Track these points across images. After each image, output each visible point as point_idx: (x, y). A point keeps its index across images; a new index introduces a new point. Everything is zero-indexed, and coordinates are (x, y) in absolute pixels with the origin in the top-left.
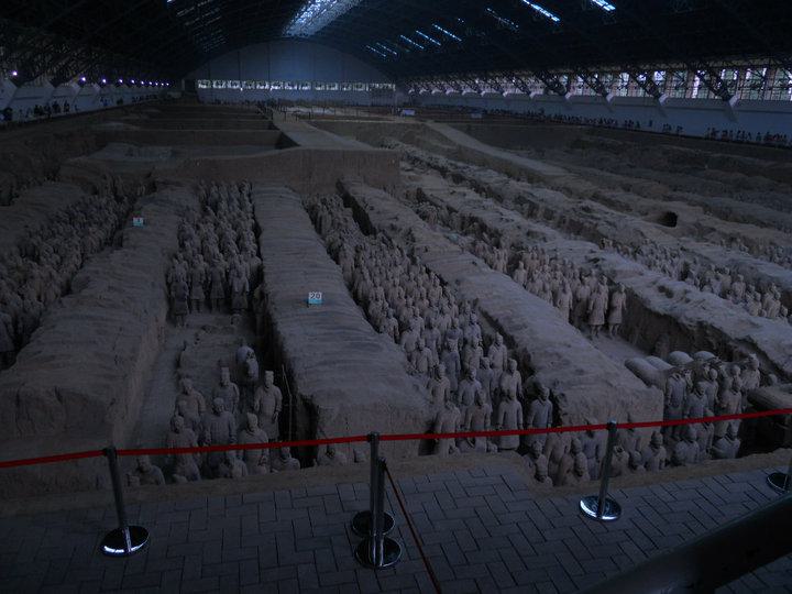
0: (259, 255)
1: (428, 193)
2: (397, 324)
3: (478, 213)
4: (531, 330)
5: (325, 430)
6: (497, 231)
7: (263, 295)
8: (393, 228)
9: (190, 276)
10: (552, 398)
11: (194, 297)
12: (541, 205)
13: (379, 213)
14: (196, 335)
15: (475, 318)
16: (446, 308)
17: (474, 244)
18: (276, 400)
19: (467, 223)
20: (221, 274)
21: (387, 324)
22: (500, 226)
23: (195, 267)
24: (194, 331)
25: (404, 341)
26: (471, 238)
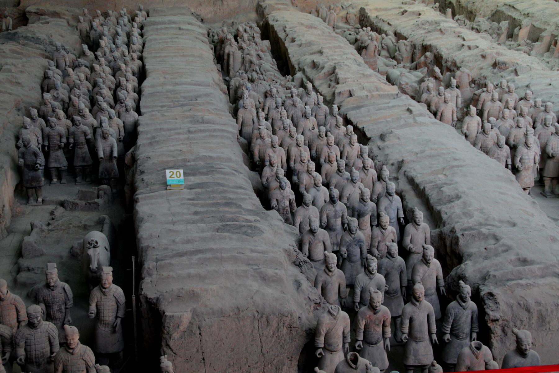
0: (138, 110)
1: (372, 14)
2: (293, 196)
3: (434, 40)
4: (465, 203)
5: (171, 343)
6: (455, 64)
7: (134, 159)
8: (314, 65)
9: (46, 137)
10: (476, 296)
11: (53, 165)
12: (525, 22)
13: (300, 46)
14: (52, 213)
15: (393, 186)
16: (357, 174)
17: (422, 81)
18: (117, 302)
19: (418, 52)
20: (85, 134)
21: (279, 197)
22: (458, 56)
23: (51, 127)
24: (51, 207)
25: (298, 220)
26: (419, 74)
